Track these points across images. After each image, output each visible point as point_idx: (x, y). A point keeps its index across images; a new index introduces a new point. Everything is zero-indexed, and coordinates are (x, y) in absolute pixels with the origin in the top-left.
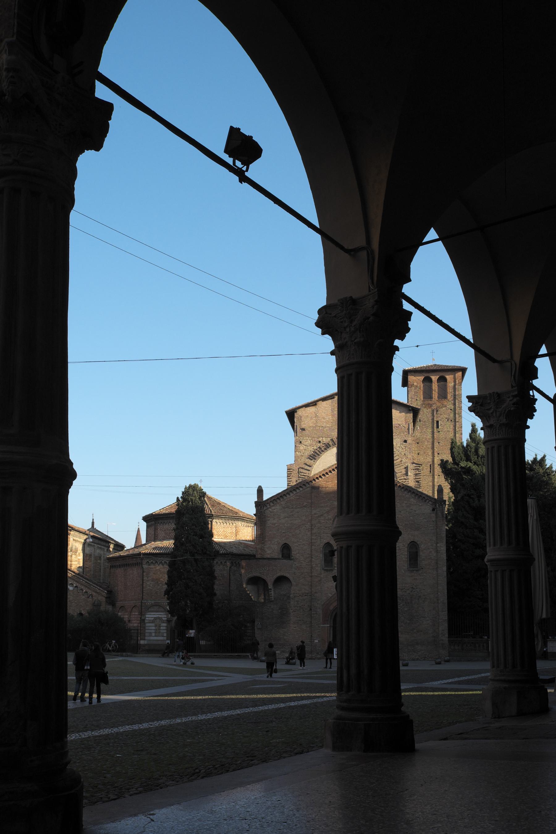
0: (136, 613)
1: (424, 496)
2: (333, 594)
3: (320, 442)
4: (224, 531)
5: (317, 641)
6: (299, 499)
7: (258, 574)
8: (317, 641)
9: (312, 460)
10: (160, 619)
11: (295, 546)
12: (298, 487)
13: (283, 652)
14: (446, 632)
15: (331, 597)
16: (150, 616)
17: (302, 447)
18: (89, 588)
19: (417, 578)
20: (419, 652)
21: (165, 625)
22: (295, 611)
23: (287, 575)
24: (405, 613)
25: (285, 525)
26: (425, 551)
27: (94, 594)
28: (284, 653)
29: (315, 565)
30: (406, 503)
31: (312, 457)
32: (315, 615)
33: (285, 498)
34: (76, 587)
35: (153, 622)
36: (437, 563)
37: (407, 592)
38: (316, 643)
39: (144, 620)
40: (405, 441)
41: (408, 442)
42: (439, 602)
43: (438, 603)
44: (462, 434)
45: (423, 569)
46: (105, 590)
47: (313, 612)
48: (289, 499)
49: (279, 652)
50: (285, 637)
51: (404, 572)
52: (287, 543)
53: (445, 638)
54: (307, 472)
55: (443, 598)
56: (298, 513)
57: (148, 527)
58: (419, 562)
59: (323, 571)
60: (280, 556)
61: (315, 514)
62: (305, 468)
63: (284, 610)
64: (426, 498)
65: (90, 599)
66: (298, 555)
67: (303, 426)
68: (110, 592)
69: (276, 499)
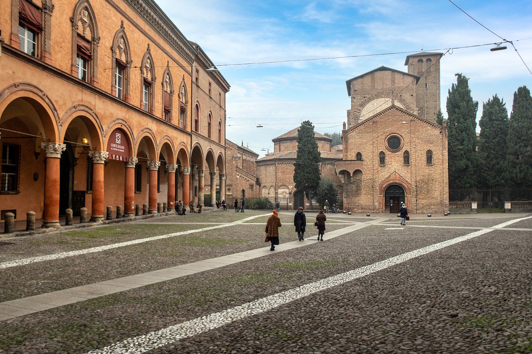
0: (272, 190)
1: (435, 125)
3: (365, 97)
7: (345, 169)
10: (286, 192)
13: (358, 209)
14: (448, 198)
16: (280, 191)
17: (355, 100)
21: (288, 195)
23: (360, 169)
27: (250, 180)
35: (282, 194)
39: (277, 193)
40: (412, 95)
53: (447, 202)
55: (446, 180)
57: (275, 145)
58: (432, 161)
59: (379, 167)
65: (248, 183)
67: (356, 89)
68: (258, 179)
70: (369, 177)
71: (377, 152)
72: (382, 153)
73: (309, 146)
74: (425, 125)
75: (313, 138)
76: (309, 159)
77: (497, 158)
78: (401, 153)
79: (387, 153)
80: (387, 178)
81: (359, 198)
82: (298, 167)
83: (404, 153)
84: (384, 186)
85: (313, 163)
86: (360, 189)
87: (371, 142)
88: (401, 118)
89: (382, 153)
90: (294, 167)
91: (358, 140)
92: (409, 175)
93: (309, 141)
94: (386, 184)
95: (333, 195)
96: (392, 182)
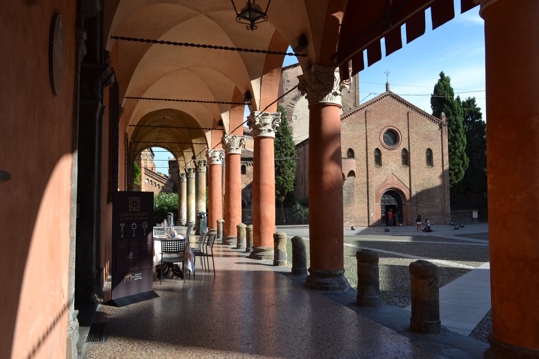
2: (381, 182)
4: (250, 144)
5: (373, 215)
6: (358, 118)
8: (373, 215)
9: (294, 101)
11: (356, 150)
12: (357, 109)
13: (350, 222)
14: (449, 207)
15: (380, 185)
18: (160, 182)
19: (432, 172)
20: (433, 220)
22: (358, 195)
24: (425, 195)
25: (350, 135)
26: (436, 155)
28: (351, 223)
29: (370, 163)
30: (424, 124)
31: (294, 99)
32: (371, 197)
33: (349, 117)
34: (151, 181)
36: (443, 163)
37: (426, 181)
38: (372, 216)
40: (349, 92)
41: (350, 93)
42: (445, 187)
43: (444, 188)
44: (359, 92)
45: (434, 166)
46: (172, 183)
47: (369, 195)
48: (351, 118)
49: (348, 223)
50: (352, 213)
51: (424, 168)
52: (351, 148)
53: (448, 210)
54: (292, 108)
56: (358, 127)
59: (375, 167)
60: (347, 157)
61: (369, 128)
62: (290, 106)
63: (350, 194)
64: (436, 121)
66: (358, 156)
67: (289, 79)
69: (343, 117)
70: (363, 181)
72: (378, 150)
74: (425, 118)
78: (399, 150)
80: (384, 183)
81: (352, 208)
84: (380, 192)
86: (353, 196)
87: (364, 137)
88: (398, 108)
89: (378, 150)
91: (348, 133)
96: (389, 187)
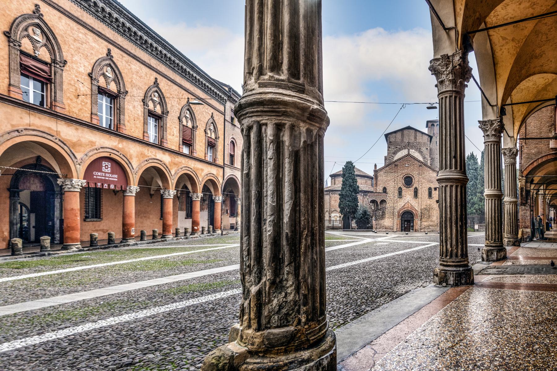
17: (390, 150)
71: (397, 187)
72: (400, 188)
73: (351, 180)
75: (354, 175)
76: (350, 191)
77: (472, 195)
78: (412, 189)
79: (403, 188)
82: (342, 196)
83: (415, 189)
85: (353, 194)
89: (400, 188)
90: (339, 197)
92: (417, 205)
93: (350, 176)
94: (402, 211)
95: (367, 218)
96: (406, 209)
